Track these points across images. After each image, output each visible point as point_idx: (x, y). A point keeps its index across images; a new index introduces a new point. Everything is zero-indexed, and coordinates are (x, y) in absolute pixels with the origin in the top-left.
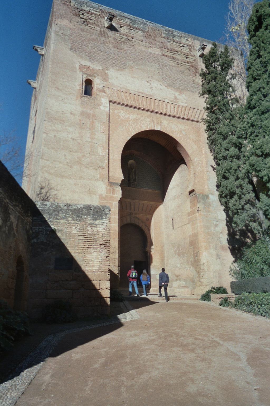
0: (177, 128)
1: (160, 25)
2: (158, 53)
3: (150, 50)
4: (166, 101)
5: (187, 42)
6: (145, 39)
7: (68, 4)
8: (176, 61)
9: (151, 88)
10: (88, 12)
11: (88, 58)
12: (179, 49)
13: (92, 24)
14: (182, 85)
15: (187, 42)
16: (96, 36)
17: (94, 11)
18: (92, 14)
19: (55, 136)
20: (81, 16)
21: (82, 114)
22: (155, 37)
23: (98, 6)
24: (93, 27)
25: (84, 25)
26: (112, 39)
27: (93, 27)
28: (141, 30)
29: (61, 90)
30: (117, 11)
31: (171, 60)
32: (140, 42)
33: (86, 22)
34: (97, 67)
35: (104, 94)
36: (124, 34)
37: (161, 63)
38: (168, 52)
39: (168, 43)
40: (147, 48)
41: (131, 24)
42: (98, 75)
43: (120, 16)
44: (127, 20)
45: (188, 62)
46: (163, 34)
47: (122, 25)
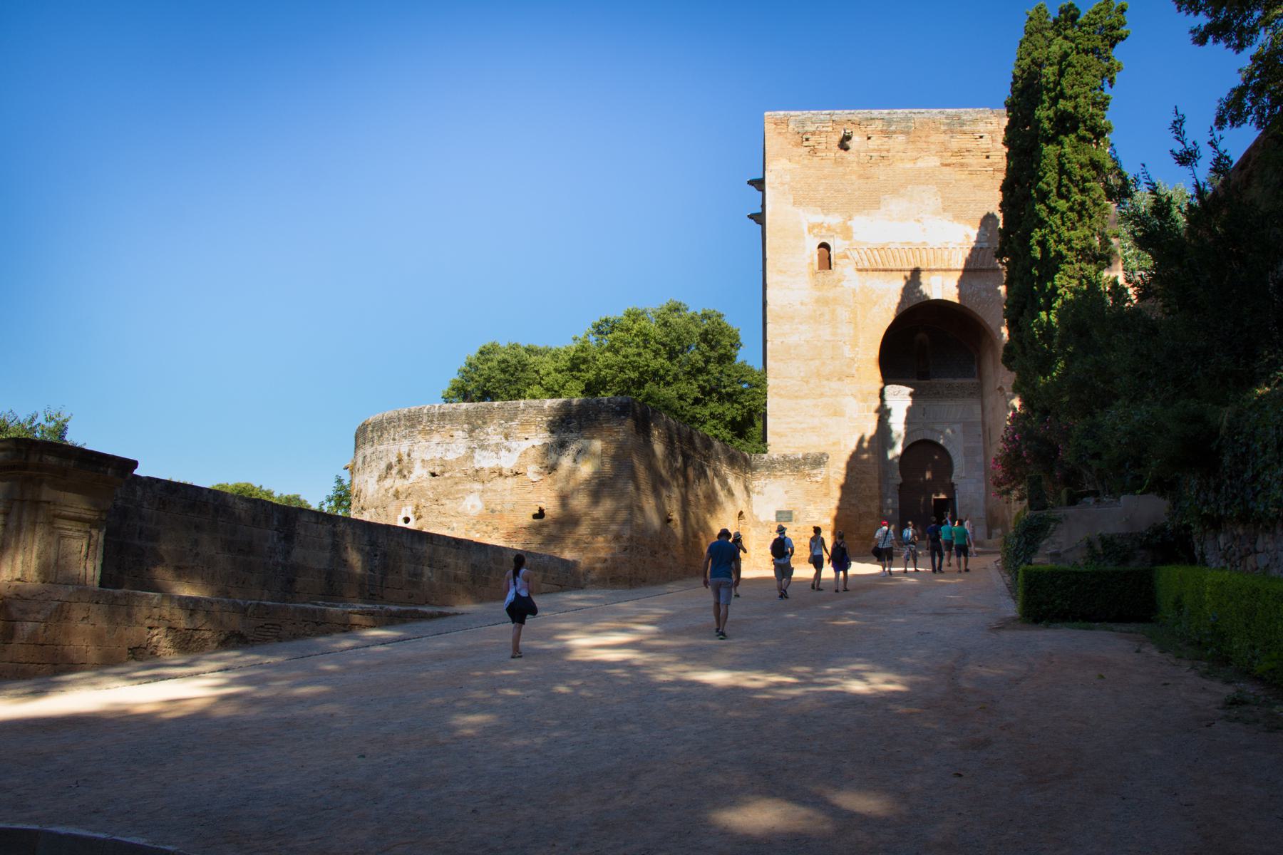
0: (971, 288)
1: (935, 111)
2: (932, 164)
3: (920, 164)
4: (950, 246)
5: (990, 127)
6: (911, 146)
7: (784, 131)
8: (969, 169)
9: (924, 230)
10: (813, 134)
11: (819, 209)
12: (971, 145)
13: (822, 151)
14: (980, 211)
15: (990, 127)
16: (830, 170)
17: (823, 127)
18: (821, 132)
19: (782, 342)
20: (806, 143)
21: (817, 301)
22: (927, 136)
23: (828, 116)
24: (824, 154)
25: (811, 158)
26: (855, 164)
27: (824, 154)
28: (902, 133)
29: (785, 272)
30: (859, 113)
31: (958, 169)
32: (901, 154)
33: (814, 151)
34: (834, 220)
35: (847, 260)
36: (874, 150)
37: (939, 181)
38: (952, 158)
39: (952, 140)
40: (915, 161)
41: (885, 128)
42: (837, 233)
43: (867, 119)
44: (877, 122)
45: (991, 165)
46: (942, 126)
47: (869, 136)
